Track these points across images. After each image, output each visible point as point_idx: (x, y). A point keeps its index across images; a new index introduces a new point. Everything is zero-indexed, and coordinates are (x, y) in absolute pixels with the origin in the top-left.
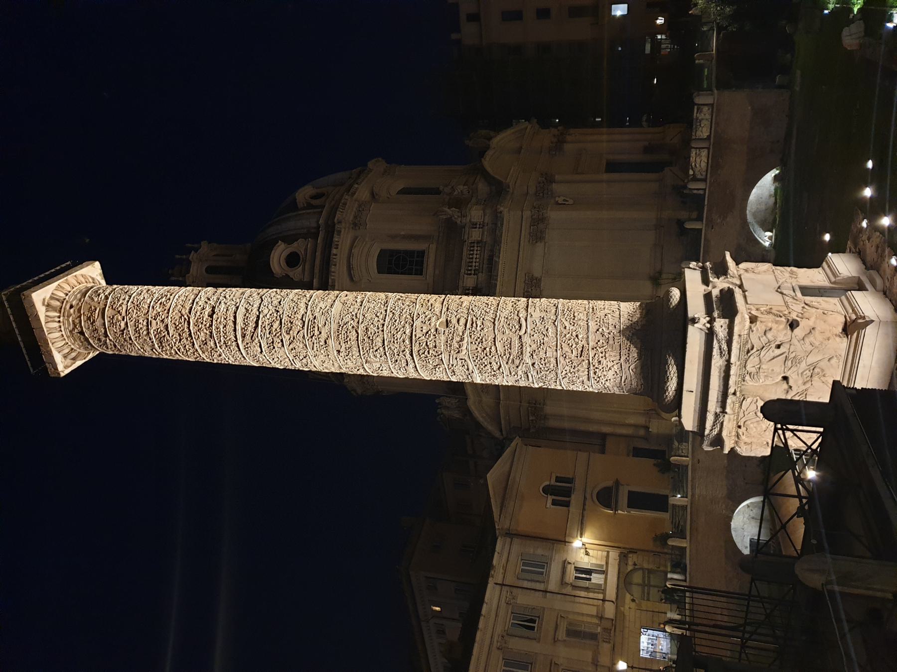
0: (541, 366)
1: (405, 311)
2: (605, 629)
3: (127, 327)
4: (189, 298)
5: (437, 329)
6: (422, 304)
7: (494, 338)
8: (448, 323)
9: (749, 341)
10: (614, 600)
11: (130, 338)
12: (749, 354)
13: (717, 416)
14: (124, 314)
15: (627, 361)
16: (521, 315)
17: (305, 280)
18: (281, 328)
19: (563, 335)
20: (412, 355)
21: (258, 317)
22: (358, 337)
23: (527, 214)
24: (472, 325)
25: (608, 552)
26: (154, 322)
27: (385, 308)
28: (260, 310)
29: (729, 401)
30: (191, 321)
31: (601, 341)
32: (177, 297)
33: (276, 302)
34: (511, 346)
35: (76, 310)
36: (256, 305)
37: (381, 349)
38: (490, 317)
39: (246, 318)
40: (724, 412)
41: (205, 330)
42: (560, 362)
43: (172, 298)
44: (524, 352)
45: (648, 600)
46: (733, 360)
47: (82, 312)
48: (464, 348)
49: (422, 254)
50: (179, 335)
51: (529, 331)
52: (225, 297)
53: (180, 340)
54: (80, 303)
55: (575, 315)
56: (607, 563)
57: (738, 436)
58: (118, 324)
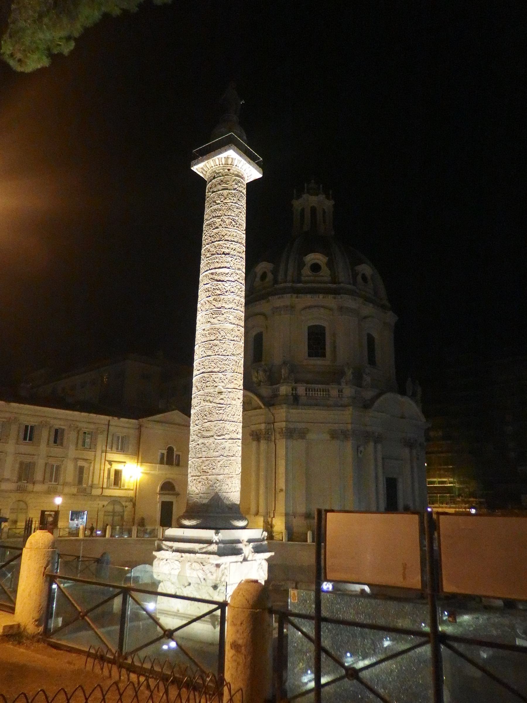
0: (197, 449)
1: (228, 366)
2: (85, 489)
3: (217, 204)
4: (235, 238)
5: (216, 387)
6: (233, 376)
7: (212, 421)
8: (220, 393)
9: (206, 564)
10: (103, 494)
11: (211, 207)
12: (201, 564)
13: (171, 547)
14: (224, 201)
15: (201, 497)
16: (226, 435)
17: (302, 278)
18: (216, 295)
19: (214, 461)
20: (203, 373)
21: (223, 281)
22: (212, 340)
23: (349, 427)
24: (220, 407)
25: (133, 490)
26: (220, 220)
27: (229, 355)
28: (227, 282)
29: (178, 554)
30: (220, 242)
31: (211, 482)
32: (236, 230)
33: (232, 290)
34: (208, 431)
35: (227, 173)
36: (230, 279)
37: (205, 355)
38: (225, 417)
39: (222, 274)
40: (174, 551)
41: (215, 251)
42: (200, 460)
43: (235, 228)
44: (204, 439)
45: (105, 515)
46: (197, 555)
47: (225, 177)
48: (206, 403)
49: (323, 355)
50: (213, 236)
51: (217, 441)
52: (236, 259)
53: (210, 236)
54: (231, 174)
55: (227, 467)
56: (126, 489)
57: (162, 559)
58: (219, 199)
